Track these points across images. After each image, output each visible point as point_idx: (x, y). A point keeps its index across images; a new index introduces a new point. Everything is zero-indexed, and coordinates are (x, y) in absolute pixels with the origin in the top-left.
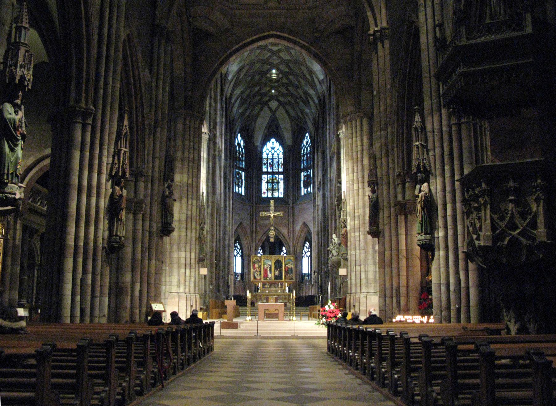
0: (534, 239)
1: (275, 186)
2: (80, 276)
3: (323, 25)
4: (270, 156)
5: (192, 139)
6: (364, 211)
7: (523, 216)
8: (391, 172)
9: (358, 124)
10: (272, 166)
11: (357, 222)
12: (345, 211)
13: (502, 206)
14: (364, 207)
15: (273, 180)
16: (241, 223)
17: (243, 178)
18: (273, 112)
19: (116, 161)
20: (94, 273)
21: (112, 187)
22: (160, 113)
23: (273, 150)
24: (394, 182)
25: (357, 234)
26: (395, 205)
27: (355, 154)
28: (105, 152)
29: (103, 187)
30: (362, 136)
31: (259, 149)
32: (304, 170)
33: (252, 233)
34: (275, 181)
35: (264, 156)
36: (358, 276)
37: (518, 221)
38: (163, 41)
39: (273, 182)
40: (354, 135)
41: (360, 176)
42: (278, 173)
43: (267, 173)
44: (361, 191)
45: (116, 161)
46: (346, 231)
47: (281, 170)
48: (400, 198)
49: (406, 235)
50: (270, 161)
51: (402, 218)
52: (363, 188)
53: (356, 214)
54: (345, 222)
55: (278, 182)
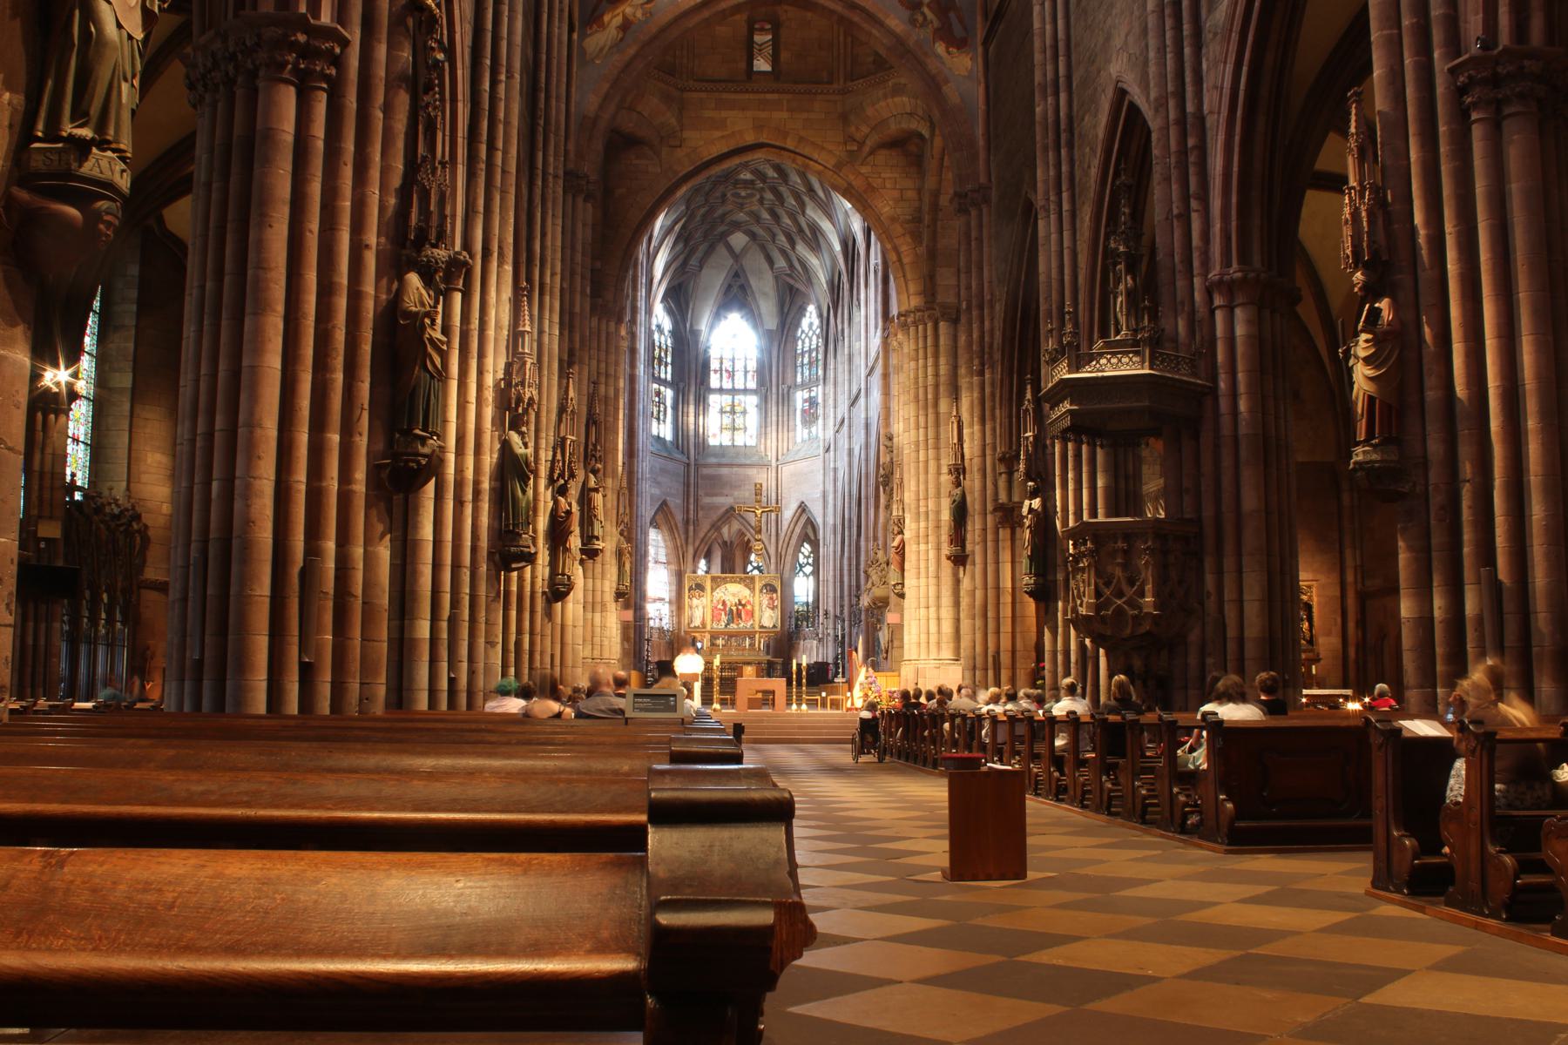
0: (1140, 608)
1: (739, 422)
2: (513, 638)
3: (865, 129)
4: (727, 355)
5: (603, 355)
6: (939, 505)
7: (1131, 582)
8: (988, 452)
9: (929, 332)
10: (732, 375)
11: (922, 524)
12: (902, 501)
13: (1109, 569)
14: (938, 495)
15: (733, 406)
16: (664, 503)
17: (669, 403)
18: (736, 257)
19: (559, 457)
20: (532, 633)
21: (556, 502)
22: (577, 338)
23: (732, 340)
24: (994, 469)
25: (923, 547)
26: (995, 510)
27: (921, 391)
28: (543, 443)
29: (542, 498)
30: (936, 356)
31: (703, 338)
32: (804, 386)
33: (687, 522)
34: (738, 409)
35: (714, 354)
36: (923, 629)
37: (1125, 587)
38: (580, 201)
39: (733, 412)
40: (921, 352)
41: (931, 434)
42: (745, 391)
43: (721, 391)
44: (932, 464)
45: (559, 457)
46: (903, 541)
47: (752, 385)
48: (1003, 498)
49: (1013, 562)
50: (727, 365)
51: (1004, 534)
52: (938, 459)
53: (922, 509)
54: (900, 522)
55: (744, 412)
